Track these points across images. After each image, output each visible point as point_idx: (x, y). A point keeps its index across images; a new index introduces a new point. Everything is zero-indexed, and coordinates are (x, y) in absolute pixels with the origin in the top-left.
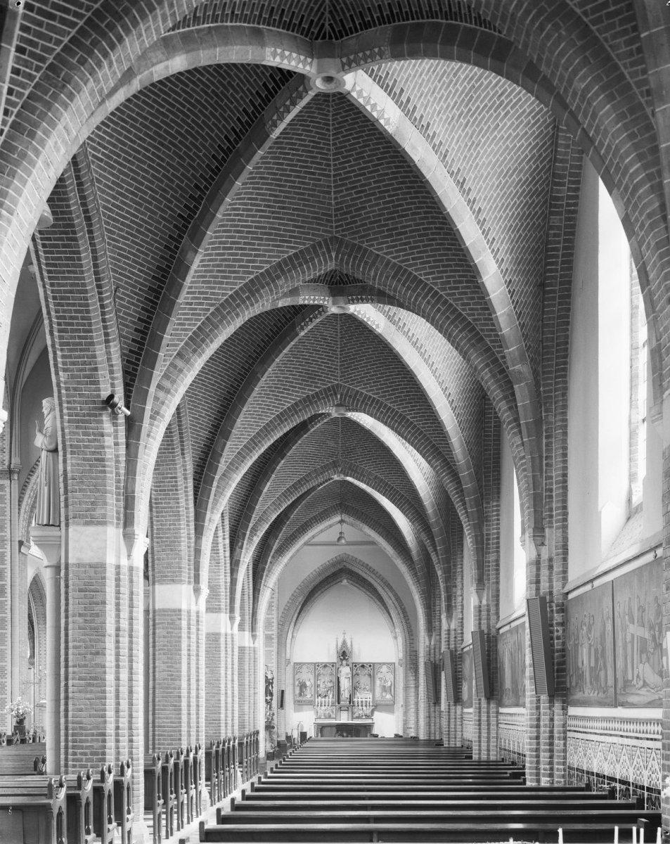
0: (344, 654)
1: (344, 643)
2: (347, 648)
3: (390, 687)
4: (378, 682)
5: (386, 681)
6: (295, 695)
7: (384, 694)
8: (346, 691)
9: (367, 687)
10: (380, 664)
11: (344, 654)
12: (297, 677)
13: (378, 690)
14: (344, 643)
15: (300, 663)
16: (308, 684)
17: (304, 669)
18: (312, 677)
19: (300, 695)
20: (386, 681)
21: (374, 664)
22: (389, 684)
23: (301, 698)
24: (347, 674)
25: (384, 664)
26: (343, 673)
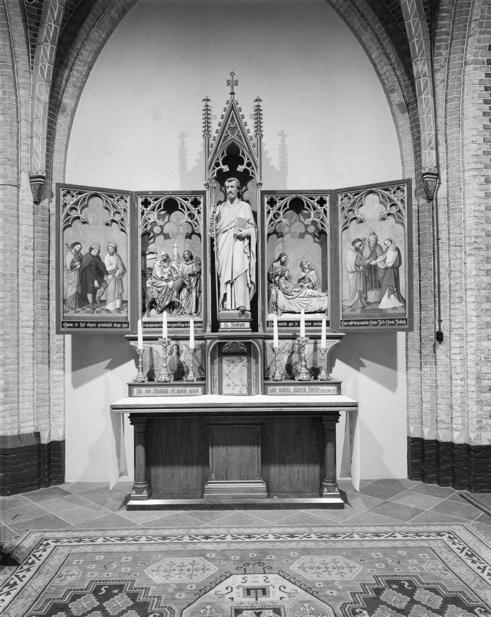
0: (233, 156)
1: (233, 111)
2: (243, 135)
3: (396, 268)
4: (348, 257)
5: (376, 250)
6: (61, 301)
7: (372, 296)
8: (240, 285)
9: (312, 275)
10: (356, 191)
11: (233, 156)
12: (70, 235)
13: (350, 284)
14: (233, 111)
15: (81, 190)
16: (109, 262)
17: (96, 210)
18: (121, 239)
19: (81, 299)
20: (376, 250)
21: (334, 193)
22: (391, 257)
23: (83, 314)
24: (242, 223)
25: (370, 189)
26: (224, 222)
